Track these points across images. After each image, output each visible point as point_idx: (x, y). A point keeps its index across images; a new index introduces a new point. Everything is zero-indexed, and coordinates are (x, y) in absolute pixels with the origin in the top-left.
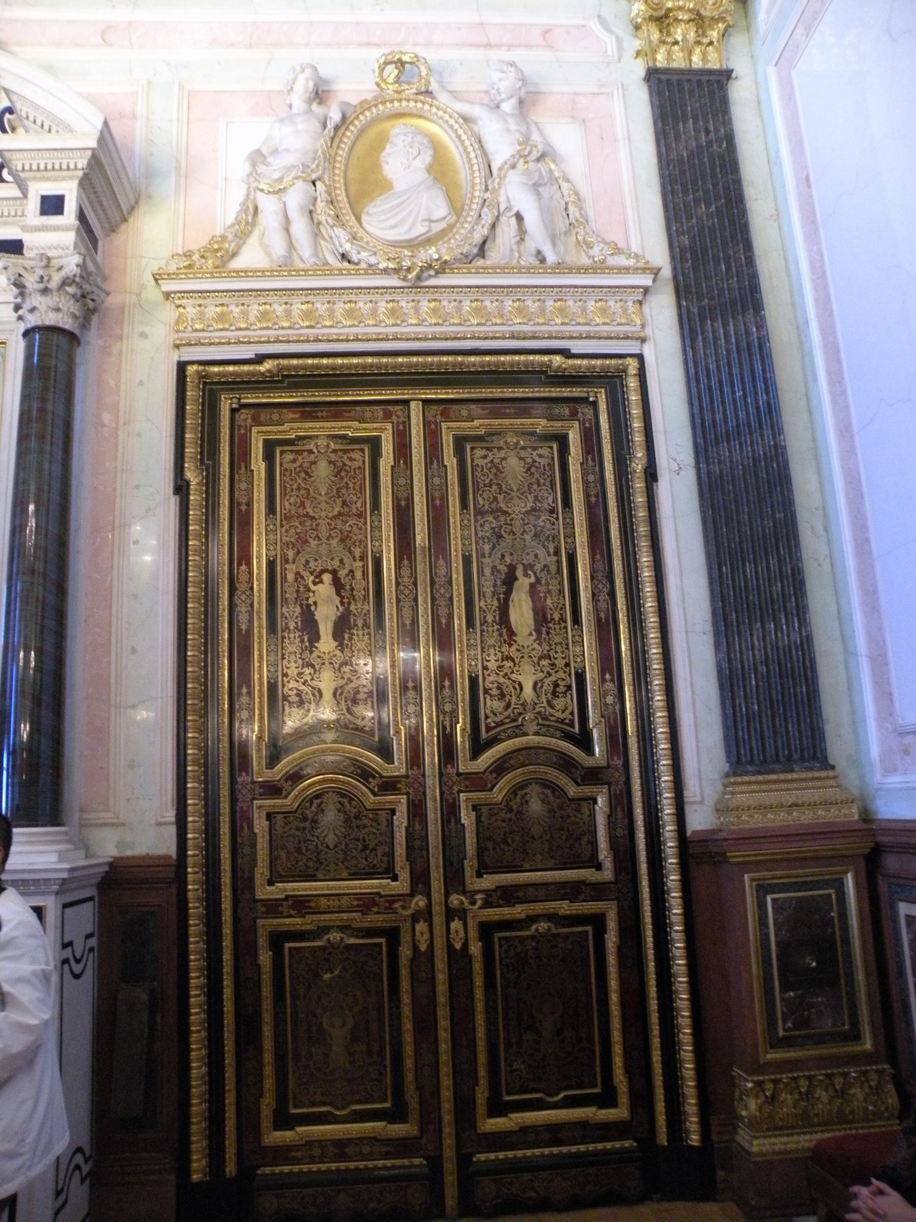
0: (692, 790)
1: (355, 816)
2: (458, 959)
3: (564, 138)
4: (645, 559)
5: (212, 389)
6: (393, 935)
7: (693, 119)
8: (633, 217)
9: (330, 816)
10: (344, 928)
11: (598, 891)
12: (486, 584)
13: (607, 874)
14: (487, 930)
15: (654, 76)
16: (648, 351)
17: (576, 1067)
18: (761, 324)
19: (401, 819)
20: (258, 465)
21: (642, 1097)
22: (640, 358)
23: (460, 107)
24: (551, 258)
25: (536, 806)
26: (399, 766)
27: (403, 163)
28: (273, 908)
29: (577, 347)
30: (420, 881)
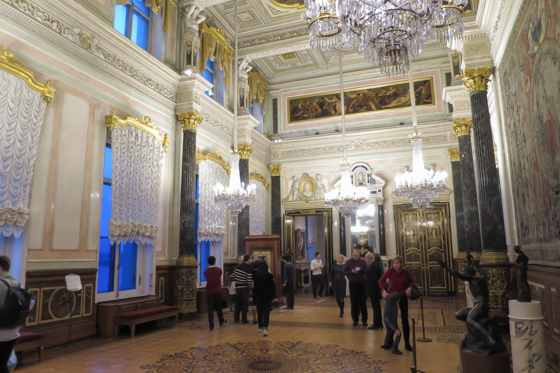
1: (415, 255)
2: (427, 271)
6: (420, 268)
9: (413, 256)
14: (430, 268)
17: (441, 283)
21: (448, 286)
28: (407, 265)
30: (423, 262)
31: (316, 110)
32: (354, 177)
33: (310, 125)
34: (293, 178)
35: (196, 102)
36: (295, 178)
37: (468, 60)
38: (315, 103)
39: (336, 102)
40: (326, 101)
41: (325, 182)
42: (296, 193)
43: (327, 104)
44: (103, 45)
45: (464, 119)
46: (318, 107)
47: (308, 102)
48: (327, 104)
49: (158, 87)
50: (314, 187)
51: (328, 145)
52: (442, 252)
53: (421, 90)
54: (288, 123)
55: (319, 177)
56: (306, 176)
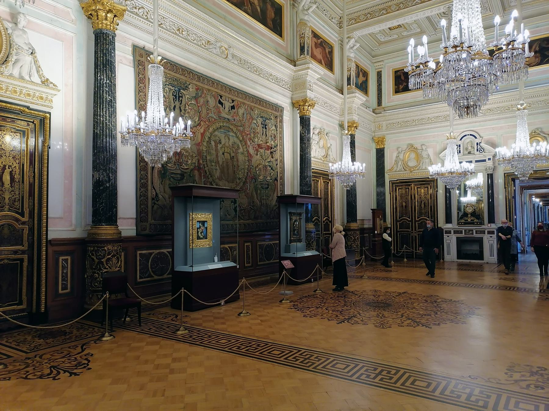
34: (398, 148)
35: (310, 90)
36: (400, 150)
41: (430, 151)
42: (400, 163)
44: (236, 53)
49: (277, 81)
50: (419, 157)
54: (393, 95)
55: (424, 148)
56: (412, 148)
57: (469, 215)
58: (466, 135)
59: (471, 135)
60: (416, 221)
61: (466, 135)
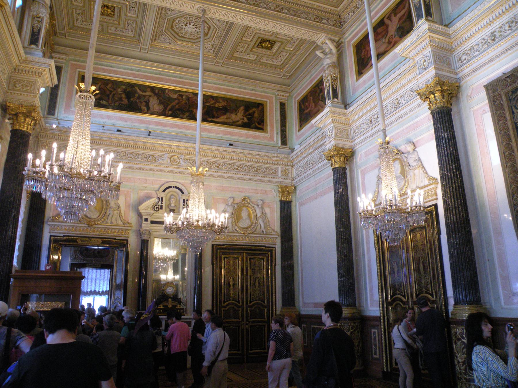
0: (277, 309)
2: (247, 330)
3: (267, 210)
4: (274, 277)
5: (217, 249)
6: (239, 327)
7: (286, 208)
8: (276, 225)
10: (233, 326)
11: (265, 322)
12: (252, 279)
13: (266, 320)
14: (251, 326)
15: (281, 201)
16: (276, 247)
18: (292, 243)
19: (240, 311)
20: (223, 261)
22: (275, 247)
23: (253, 205)
24: (265, 232)
25: (257, 310)
26: (240, 304)
27: (244, 214)
29: (267, 245)
30: (243, 320)
31: (121, 99)
32: (164, 199)
33: (108, 117)
37: (438, 69)
38: (119, 90)
39: (150, 96)
40: (136, 92)
43: (137, 95)
45: (343, 149)
46: (123, 96)
47: (110, 85)
48: (137, 95)
51: (132, 150)
52: (265, 307)
53: (254, 112)
57: (170, 300)
58: (170, 187)
59: (177, 188)
60: (248, 307)
61: (170, 187)
